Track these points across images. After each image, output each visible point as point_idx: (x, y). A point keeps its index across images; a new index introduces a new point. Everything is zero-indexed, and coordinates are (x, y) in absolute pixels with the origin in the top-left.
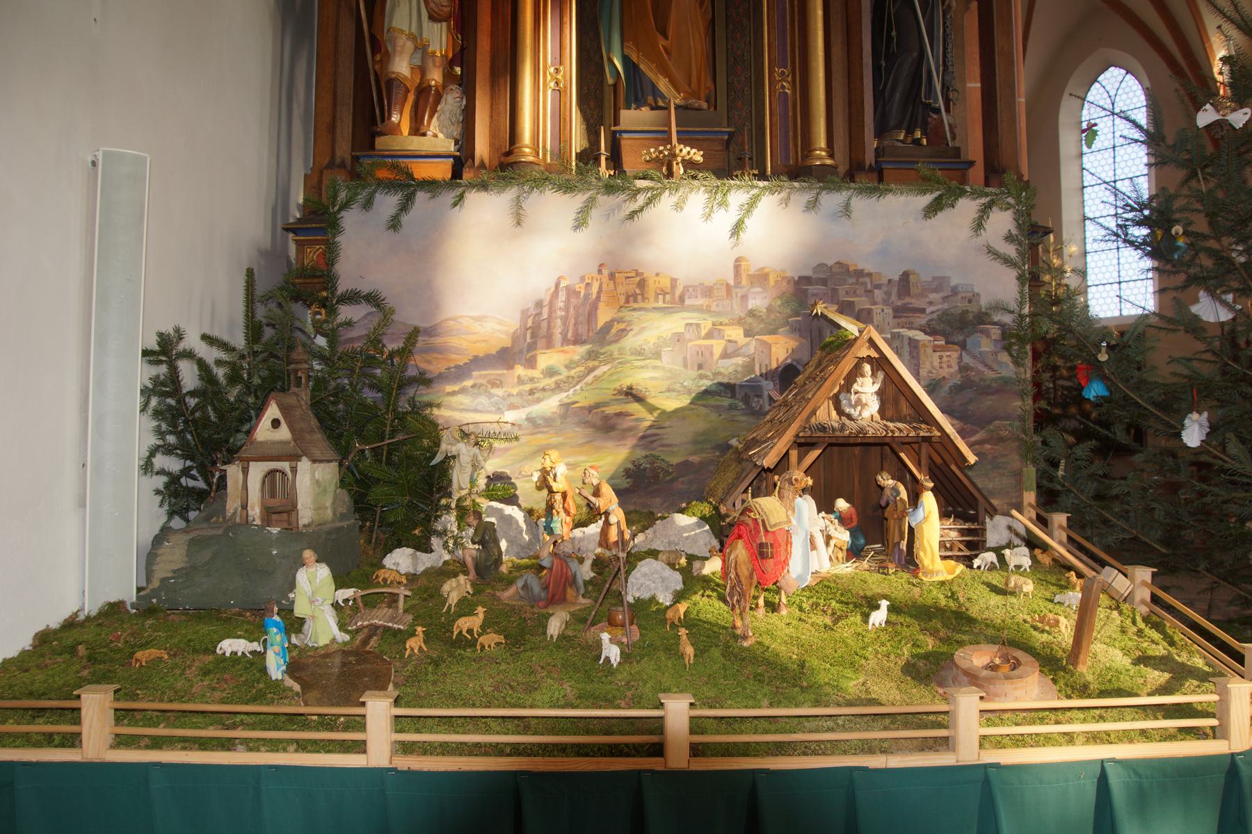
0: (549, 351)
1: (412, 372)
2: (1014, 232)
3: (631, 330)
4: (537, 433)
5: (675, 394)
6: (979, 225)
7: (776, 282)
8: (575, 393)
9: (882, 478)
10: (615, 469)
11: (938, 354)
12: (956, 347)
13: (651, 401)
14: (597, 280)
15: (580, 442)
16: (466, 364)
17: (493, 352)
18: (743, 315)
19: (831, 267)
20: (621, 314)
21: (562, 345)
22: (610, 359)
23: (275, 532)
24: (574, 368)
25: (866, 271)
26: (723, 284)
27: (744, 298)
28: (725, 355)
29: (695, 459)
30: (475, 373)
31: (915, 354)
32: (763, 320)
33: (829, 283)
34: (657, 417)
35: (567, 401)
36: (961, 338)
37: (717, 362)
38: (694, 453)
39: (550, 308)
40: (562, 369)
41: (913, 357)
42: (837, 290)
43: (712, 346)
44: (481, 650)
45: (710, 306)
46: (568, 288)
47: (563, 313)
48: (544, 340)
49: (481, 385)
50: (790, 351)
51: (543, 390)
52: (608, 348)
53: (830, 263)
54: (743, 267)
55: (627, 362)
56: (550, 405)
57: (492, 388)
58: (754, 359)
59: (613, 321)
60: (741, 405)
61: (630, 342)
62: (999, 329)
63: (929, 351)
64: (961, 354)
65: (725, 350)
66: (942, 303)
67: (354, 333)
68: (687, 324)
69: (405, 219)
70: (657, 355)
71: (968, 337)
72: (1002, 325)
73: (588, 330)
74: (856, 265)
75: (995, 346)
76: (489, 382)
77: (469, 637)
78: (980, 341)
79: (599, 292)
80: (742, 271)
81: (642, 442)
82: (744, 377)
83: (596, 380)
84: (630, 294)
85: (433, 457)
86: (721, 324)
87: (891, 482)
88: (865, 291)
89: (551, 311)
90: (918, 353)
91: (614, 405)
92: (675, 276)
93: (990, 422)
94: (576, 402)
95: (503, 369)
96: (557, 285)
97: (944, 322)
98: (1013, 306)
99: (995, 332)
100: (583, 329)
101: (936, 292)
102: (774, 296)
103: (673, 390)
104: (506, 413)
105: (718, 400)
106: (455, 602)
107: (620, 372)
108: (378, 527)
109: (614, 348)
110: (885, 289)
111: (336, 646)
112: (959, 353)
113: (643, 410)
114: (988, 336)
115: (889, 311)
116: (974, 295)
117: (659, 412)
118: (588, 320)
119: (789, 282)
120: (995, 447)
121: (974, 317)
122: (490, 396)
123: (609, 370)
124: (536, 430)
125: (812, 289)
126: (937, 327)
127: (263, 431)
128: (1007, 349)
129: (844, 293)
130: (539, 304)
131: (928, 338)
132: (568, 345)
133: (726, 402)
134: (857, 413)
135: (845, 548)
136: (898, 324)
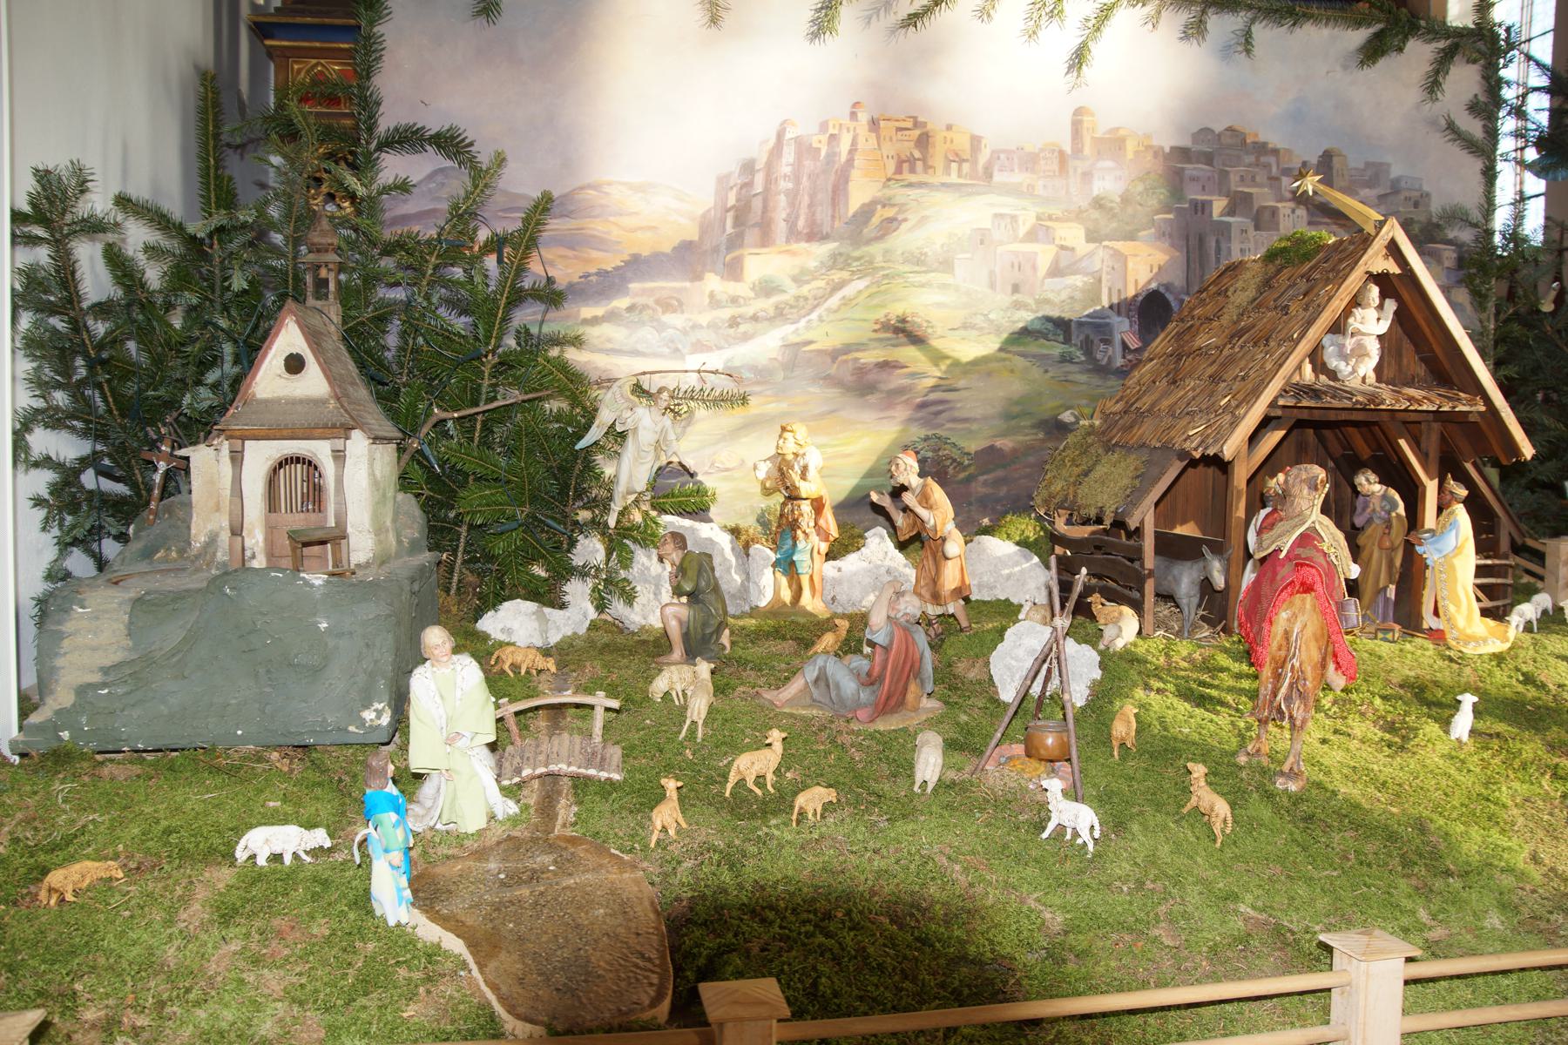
1: (531, 279)
2: (1482, 98)
3: (905, 220)
5: (974, 333)
6: (1433, 85)
7: (1137, 153)
8: (808, 328)
10: (874, 458)
13: (936, 343)
14: (848, 130)
16: (617, 269)
17: (667, 248)
18: (1084, 204)
19: (1219, 135)
21: (788, 241)
22: (868, 268)
23: (318, 582)
24: (808, 282)
26: (1053, 151)
27: (1087, 176)
28: (1056, 271)
29: (1005, 443)
30: (633, 286)
32: (1114, 216)
33: (1215, 163)
34: (945, 372)
37: (1043, 282)
38: (1003, 435)
42: (1227, 172)
44: (798, 822)
45: (1033, 187)
46: (798, 141)
49: (645, 307)
50: (1155, 270)
51: (755, 318)
53: (1218, 127)
54: (1085, 125)
56: (767, 346)
57: (664, 313)
58: (1100, 281)
60: (1080, 355)
61: (904, 240)
65: (1056, 262)
67: (410, 206)
68: (996, 215)
70: (946, 265)
73: (833, 217)
74: (1256, 135)
75: (1448, 278)
76: (657, 302)
77: (759, 792)
79: (853, 151)
80: (1085, 132)
81: (920, 415)
82: (1085, 308)
83: (845, 304)
84: (904, 157)
85: (580, 437)
86: (1050, 218)
87: (1377, 488)
88: (1271, 178)
89: (769, 180)
91: (874, 349)
92: (977, 133)
96: (780, 136)
100: (823, 214)
101: (1370, 187)
103: (973, 327)
104: (688, 358)
105: (1042, 346)
106: (703, 716)
107: (885, 292)
108: (465, 562)
109: (876, 249)
111: (499, 832)
113: (923, 358)
117: (948, 362)
118: (833, 199)
119: (1156, 155)
121: (1421, 231)
122: (661, 327)
123: (867, 287)
125: (1191, 169)
127: (269, 380)
129: (1238, 178)
130: (748, 167)
132: (798, 241)
133: (1056, 349)
134: (1350, 369)
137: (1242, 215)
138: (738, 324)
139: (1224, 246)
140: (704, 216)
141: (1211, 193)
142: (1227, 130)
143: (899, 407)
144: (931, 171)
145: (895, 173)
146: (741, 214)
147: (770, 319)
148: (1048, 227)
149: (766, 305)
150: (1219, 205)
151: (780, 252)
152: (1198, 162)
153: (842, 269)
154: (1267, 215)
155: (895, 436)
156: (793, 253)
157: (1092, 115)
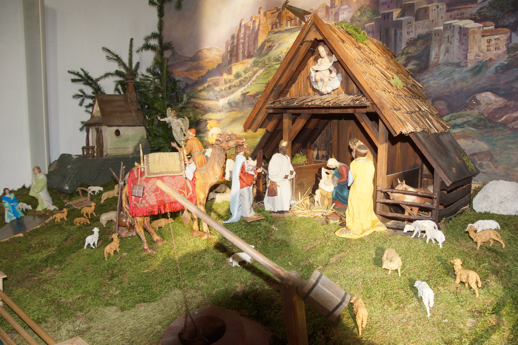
0: (237, 63)
3: (274, 46)
4: (232, 111)
8: (248, 88)
11: (486, 38)
20: (269, 37)
21: (243, 59)
24: (247, 72)
27: (337, 14)
30: (208, 79)
31: (464, 41)
35: (244, 92)
39: (238, 38)
40: (243, 73)
41: (462, 44)
46: (245, 25)
48: (235, 57)
49: (211, 85)
51: (235, 86)
52: (263, 58)
55: (272, 66)
56: (237, 95)
59: (265, 41)
63: (478, 36)
73: (254, 49)
76: (213, 84)
79: (259, 25)
84: (274, 23)
89: (238, 41)
90: (467, 40)
94: (248, 92)
95: (219, 76)
100: (251, 49)
102: (356, 9)
104: (220, 100)
109: (266, 58)
118: (254, 43)
123: (263, 72)
124: (231, 110)
130: (233, 37)
132: (245, 59)
135: (330, 196)
136: (451, 16)
137: (408, 15)
138: (231, 88)
139: (398, 32)
140: (223, 55)
141: (392, 8)
144: (281, 26)
145: (271, 30)
146: (231, 51)
147: (238, 86)
150: (396, 13)
151: (241, 64)
153: (256, 67)
156: (243, 63)
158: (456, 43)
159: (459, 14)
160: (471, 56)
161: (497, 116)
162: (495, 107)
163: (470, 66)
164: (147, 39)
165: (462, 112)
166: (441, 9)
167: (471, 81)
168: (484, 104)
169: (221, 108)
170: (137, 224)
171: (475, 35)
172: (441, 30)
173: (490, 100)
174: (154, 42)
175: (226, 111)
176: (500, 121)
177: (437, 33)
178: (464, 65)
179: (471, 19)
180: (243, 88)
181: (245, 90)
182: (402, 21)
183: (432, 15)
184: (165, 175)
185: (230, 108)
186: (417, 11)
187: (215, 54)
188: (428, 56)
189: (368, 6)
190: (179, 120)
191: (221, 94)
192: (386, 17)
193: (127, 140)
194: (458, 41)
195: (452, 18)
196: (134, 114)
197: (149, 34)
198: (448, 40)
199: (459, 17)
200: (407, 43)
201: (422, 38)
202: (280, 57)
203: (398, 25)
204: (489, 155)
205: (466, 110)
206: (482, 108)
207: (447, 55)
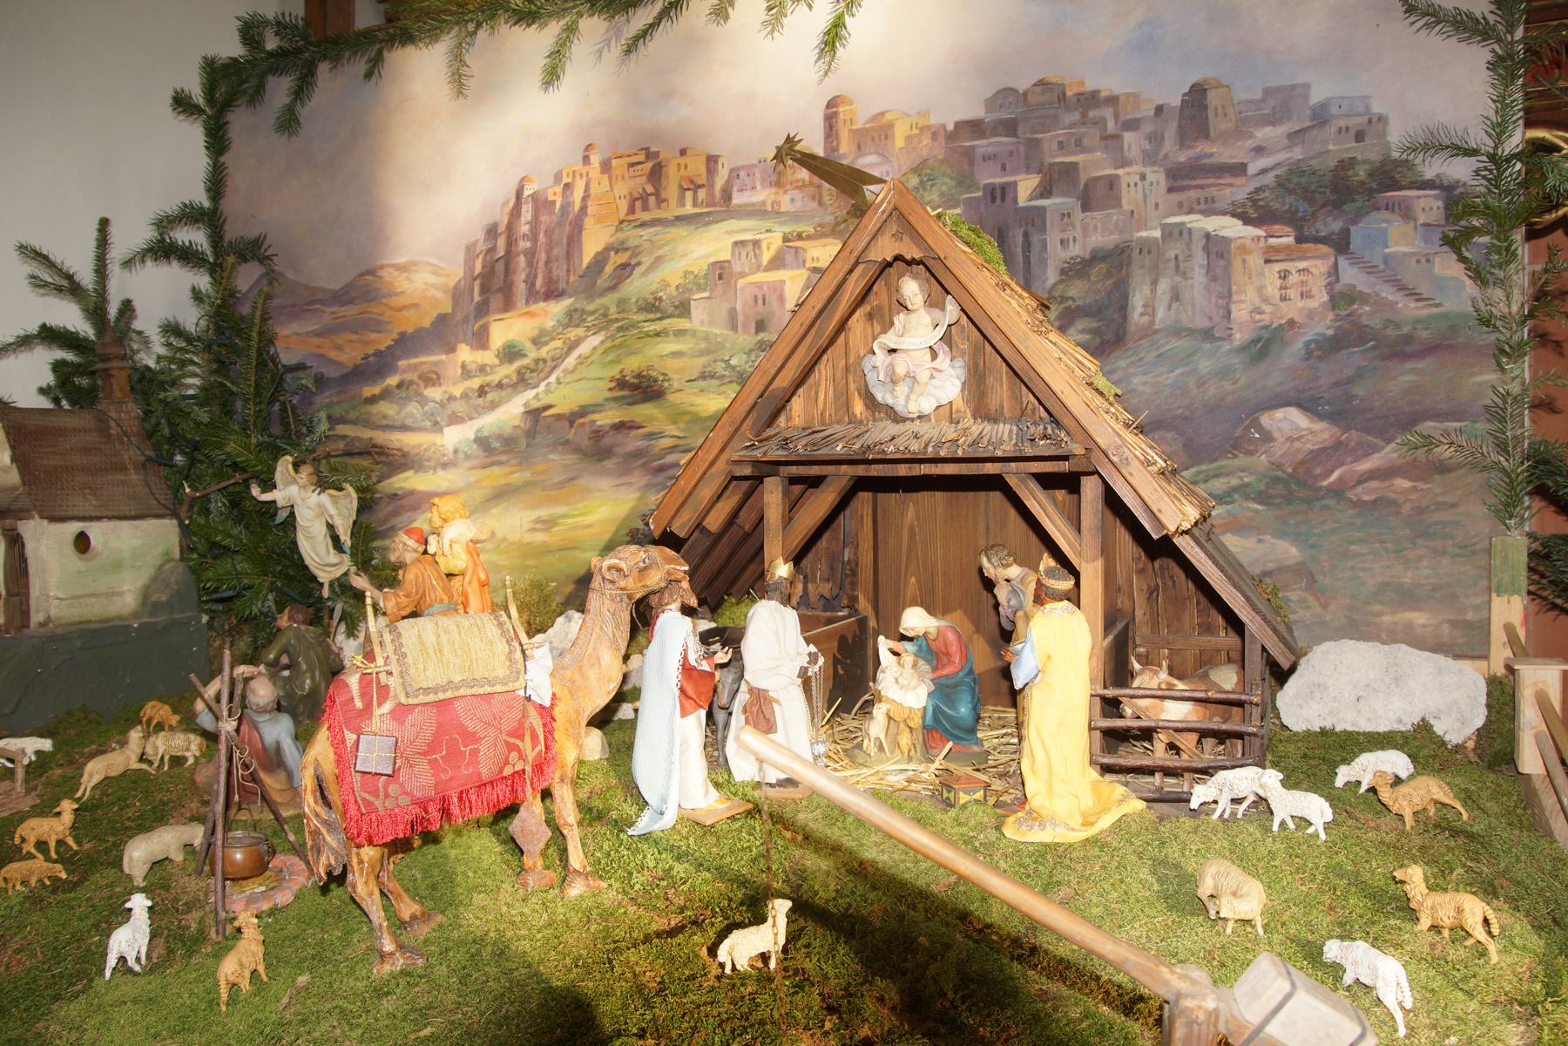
0: (508, 315)
3: (639, 264)
4: (492, 464)
5: (715, 382)
7: (909, 138)
8: (547, 392)
9: (989, 560)
10: (613, 529)
11: (1277, 267)
12: (1324, 249)
15: (557, 479)
16: (389, 347)
19: (1025, 94)
21: (527, 303)
24: (546, 343)
25: (1103, 94)
30: (402, 363)
31: (1218, 271)
33: (1020, 131)
35: (535, 404)
36: (1336, 226)
39: (509, 237)
40: (528, 346)
41: (1215, 279)
42: (1038, 141)
43: (783, 282)
45: (779, 204)
46: (534, 196)
47: (529, 244)
48: (500, 295)
49: (411, 383)
51: (500, 386)
53: (1022, 85)
54: (841, 116)
56: (510, 413)
57: (426, 387)
59: (608, 249)
62: (1436, 197)
63: (1256, 260)
64: (1335, 266)
66: (1289, 148)
68: (736, 244)
69: (304, 112)
71: (1354, 222)
72: (1447, 189)
73: (568, 271)
74: (1082, 83)
75: (1427, 240)
76: (420, 377)
78: (1384, 231)
79: (585, 198)
80: (840, 125)
83: (581, 363)
84: (636, 195)
86: (800, 237)
88: (1105, 138)
89: (511, 243)
90: (1227, 268)
92: (713, 153)
93: (1409, 422)
94: (550, 407)
95: (440, 353)
97: (1291, 192)
98: (1479, 137)
99: (1429, 206)
100: (559, 271)
101: (1273, 124)
102: (904, 169)
103: (712, 376)
104: (446, 430)
109: (609, 300)
110: (1148, 128)
112: (1333, 259)
113: (660, 416)
114: (1407, 213)
115: (1157, 177)
116: (1370, 121)
117: (687, 418)
118: (568, 252)
119: (934, 135)
120: (1421, 485)
121: (1371, 175)
123: (602, 342)
124: (490, 460)
125: (982, 145)
126: (1276, 205)
128: (1454, 243)
129: (1055, 146)
130: (492, 232)
131: (1252, 231)
132: (536, 301)
135: (916, 722)
136: (1180, 205)
137: (1063, 195)
138: (486, 393)
139: (1035, 239)
140: (455, 288)
141: (1016, 171)
142: (1035, 85)
143: (637, 472)
145: (627, 214)
146: (487, 278)
147: (514, 386)
148: (797, 249)
149: (507, 371)
150: (1026, 187)
152: (995, 135)
153: (577, 326)
154: (1101, 189)
155: (632, 504)
157: (851, 103)
158: (1199, 277)
159: (1202, 201)
160: (1240, 313)
161: (1318, 471)
162: (1311, 447)
163: (1239, 337)
164: (164, 223)
165: (1225, 462)
166: (1152, 184)
167: (1243, 379)
168: (1281, 440)
169: (451, 456)
170: (362, 869)
171: (1247, 257)
172: (1156, 238)
173: (1298, 429)
174: (195, 237)
175: (468, 464)
176: (1325, 483)
177: (1146, 247)
178: (1224, 335)
179: (1234, 215)
180: (530, 394)
181: (536, 397)
182: (1044, 208)
183: (1130, 197)
184: (462, 692)
185: (482, 454)
186: (1086, 185)
187: (426, 284)
188: (1123, 308)
189: (942, 162)
190: (325, 498)
191: (449, 412)
192: (998, 195)
193: (117, 566)
194: (1203, 271)
195: (1185, 209)
196: (134, 477)
197: (171, 206)
198: (1177, 267)
199: (1202, 207)
200: (1063, 272)
201: (1103, 259)
202: (660, 299)
203: (1034, 219)
204: (1302, 572)
205: (1235, 456)
206: (1279, 449)
207: (1175, 305)
